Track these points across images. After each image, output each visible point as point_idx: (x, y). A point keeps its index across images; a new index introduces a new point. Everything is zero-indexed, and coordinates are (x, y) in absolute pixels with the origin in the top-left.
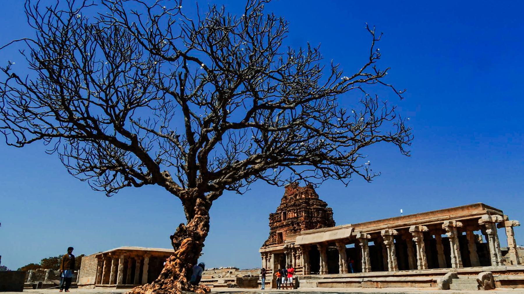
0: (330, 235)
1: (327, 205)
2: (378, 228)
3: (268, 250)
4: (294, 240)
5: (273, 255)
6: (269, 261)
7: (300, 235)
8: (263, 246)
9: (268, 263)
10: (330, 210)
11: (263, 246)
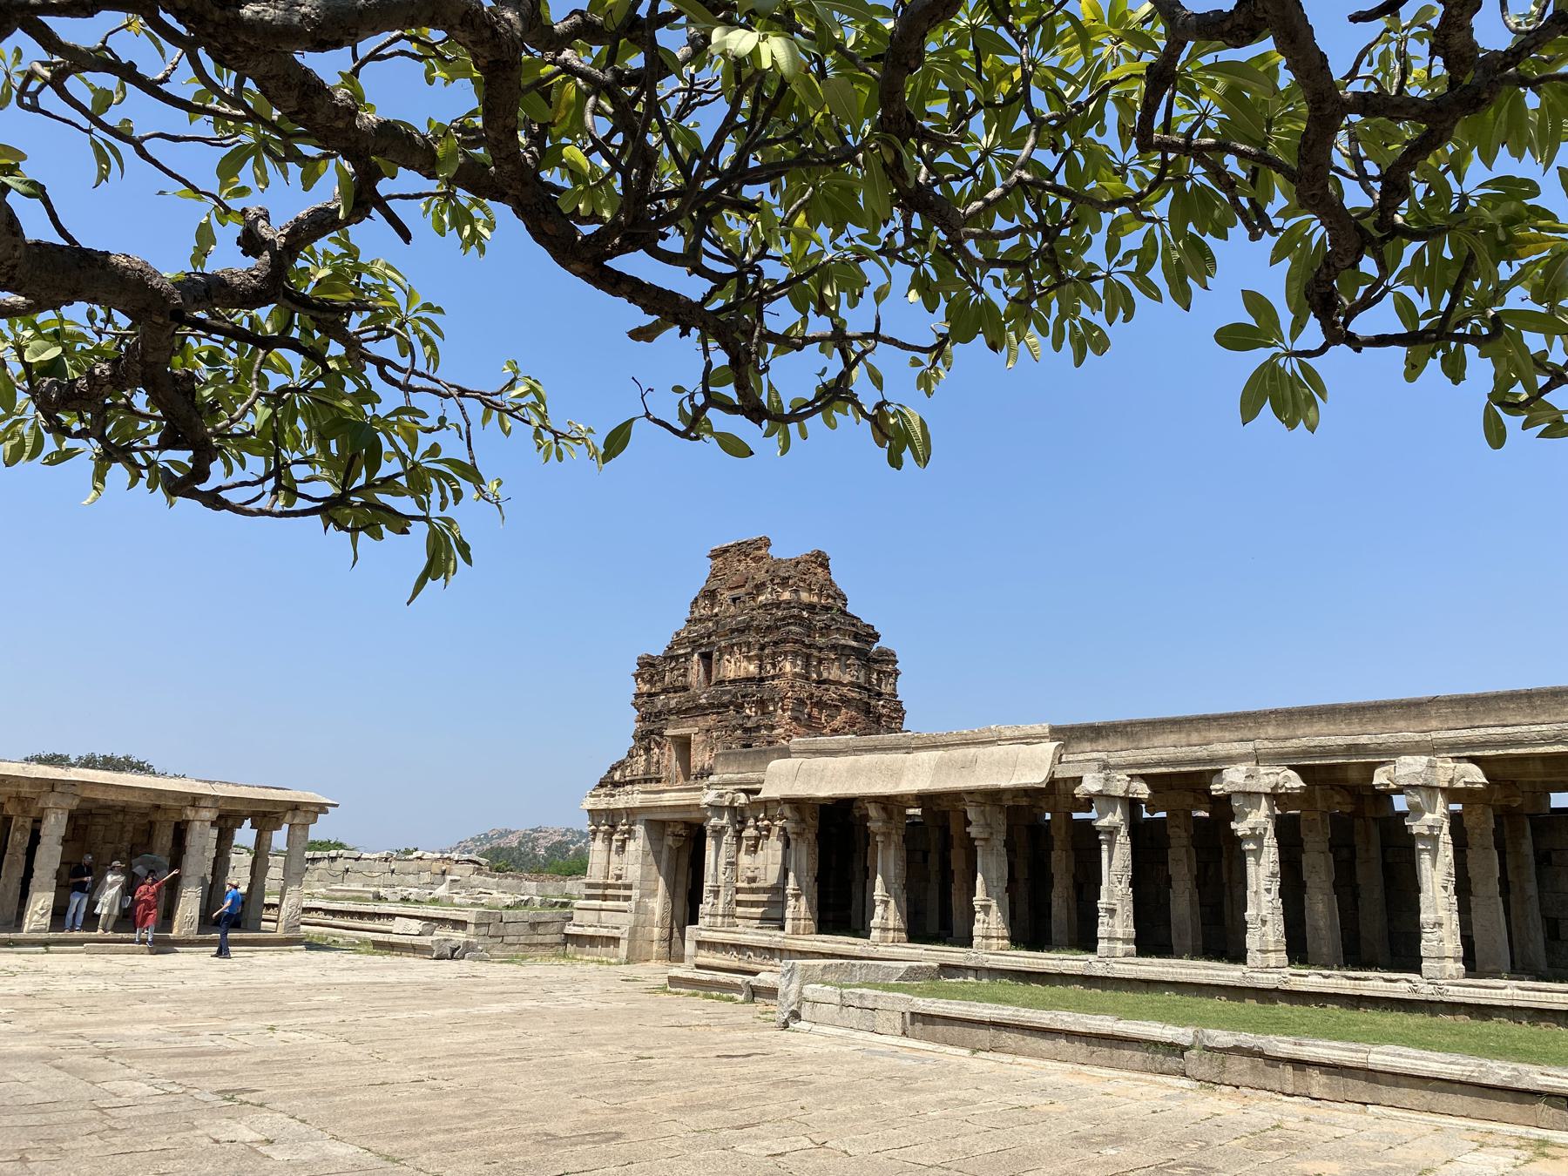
0: (939, 766)
1: (877, 637)
2: (1202, 752)
3: (621, 801)
4: (751, 775)
5: (640, 829)
6: (622, 848)
7: (786, 753)
8: (601, 785)
9: (614, 858)
10: (888, 657)
11: (601, 785)
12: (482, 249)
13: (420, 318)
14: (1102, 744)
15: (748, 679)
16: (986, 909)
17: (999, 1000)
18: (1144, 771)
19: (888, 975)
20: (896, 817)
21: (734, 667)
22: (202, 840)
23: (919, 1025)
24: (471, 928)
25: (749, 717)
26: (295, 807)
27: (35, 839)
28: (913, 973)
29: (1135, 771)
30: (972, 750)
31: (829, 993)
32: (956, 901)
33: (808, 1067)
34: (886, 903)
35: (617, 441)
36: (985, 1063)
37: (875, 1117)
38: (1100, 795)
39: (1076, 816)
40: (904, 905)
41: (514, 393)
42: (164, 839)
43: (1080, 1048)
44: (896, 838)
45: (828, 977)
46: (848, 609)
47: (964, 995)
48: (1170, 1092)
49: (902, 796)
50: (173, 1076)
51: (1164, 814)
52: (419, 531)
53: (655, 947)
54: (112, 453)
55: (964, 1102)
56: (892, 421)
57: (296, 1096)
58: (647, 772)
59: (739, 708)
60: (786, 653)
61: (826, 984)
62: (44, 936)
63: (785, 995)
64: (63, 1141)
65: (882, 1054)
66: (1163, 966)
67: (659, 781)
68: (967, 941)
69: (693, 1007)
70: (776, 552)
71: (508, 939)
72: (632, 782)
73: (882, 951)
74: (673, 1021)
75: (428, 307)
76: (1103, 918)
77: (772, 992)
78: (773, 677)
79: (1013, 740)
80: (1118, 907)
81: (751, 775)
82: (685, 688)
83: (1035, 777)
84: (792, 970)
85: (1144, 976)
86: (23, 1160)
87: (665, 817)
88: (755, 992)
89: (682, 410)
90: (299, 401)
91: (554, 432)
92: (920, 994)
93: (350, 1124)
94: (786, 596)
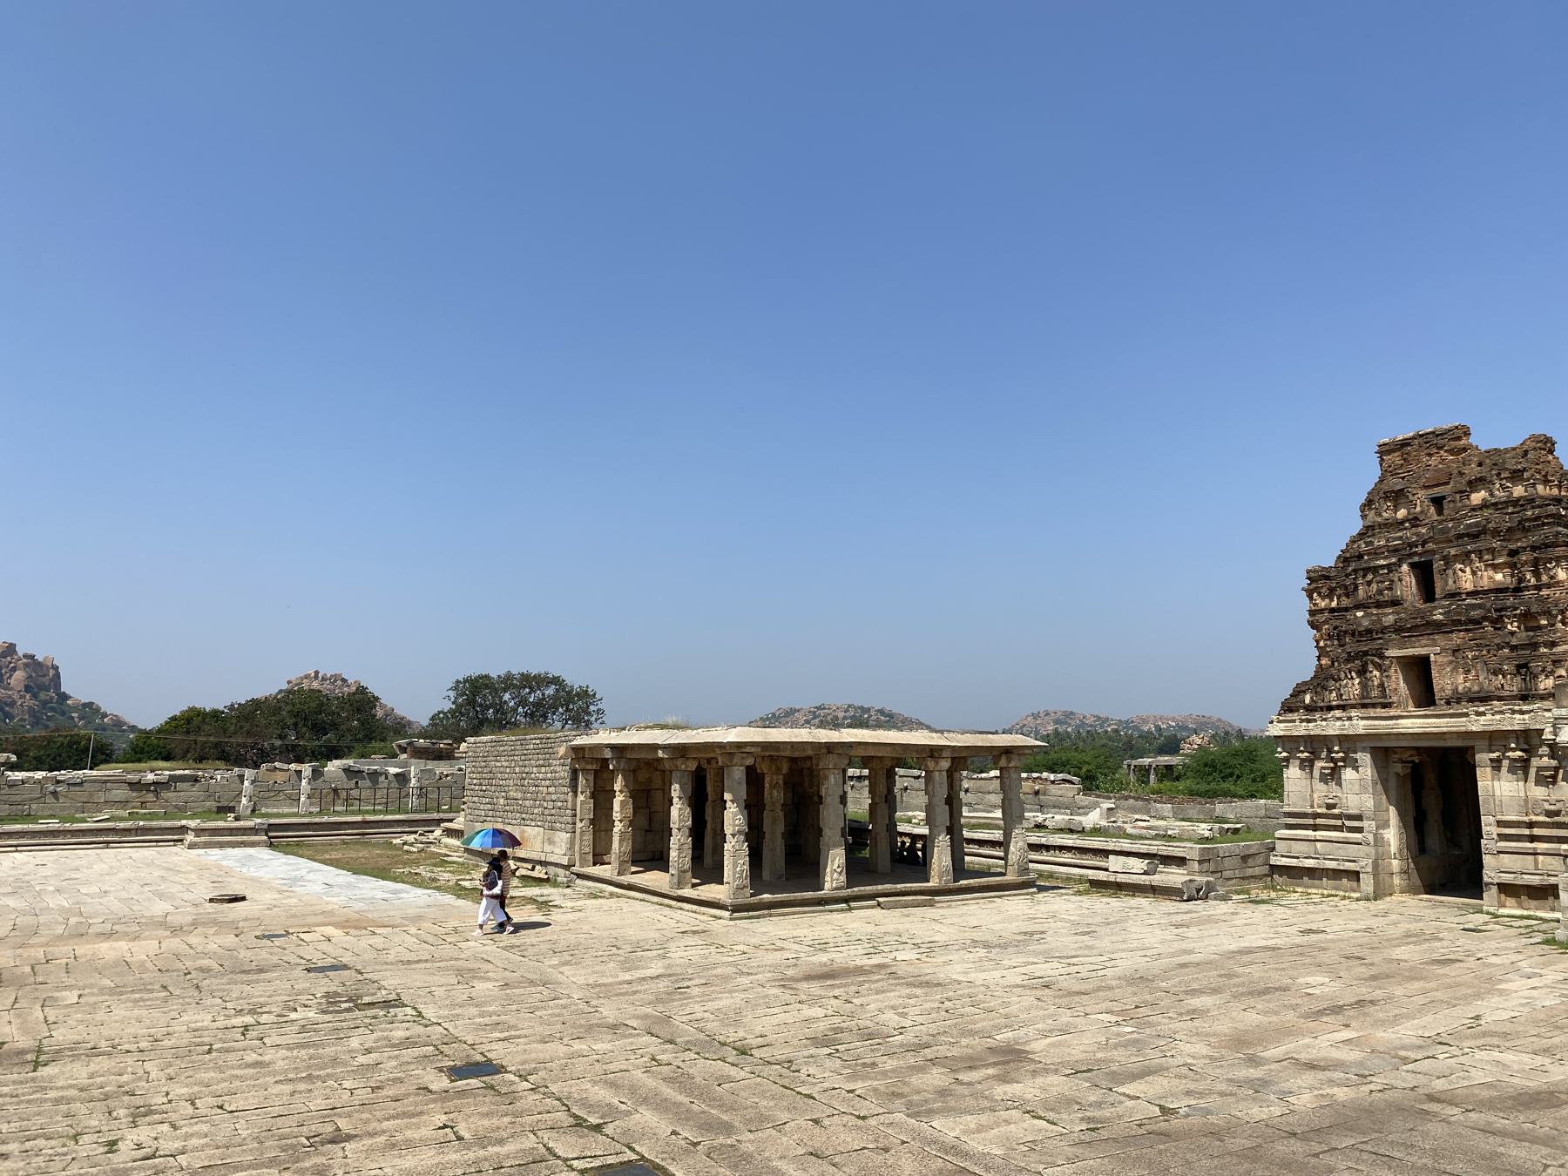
3: (1331, 726)
5: (1364, 758)
15: (1500, 590)
25: (1512, 633)
53: (1397, 880)
58: (1363, 698)
59: (1498, 623)
60: (1558, 560)
67: (1385, 706)
70: (1473, 440)
71: (1227, 874)
78: (1538, 588)
82: (1395, 603)
94: (1519, 491)
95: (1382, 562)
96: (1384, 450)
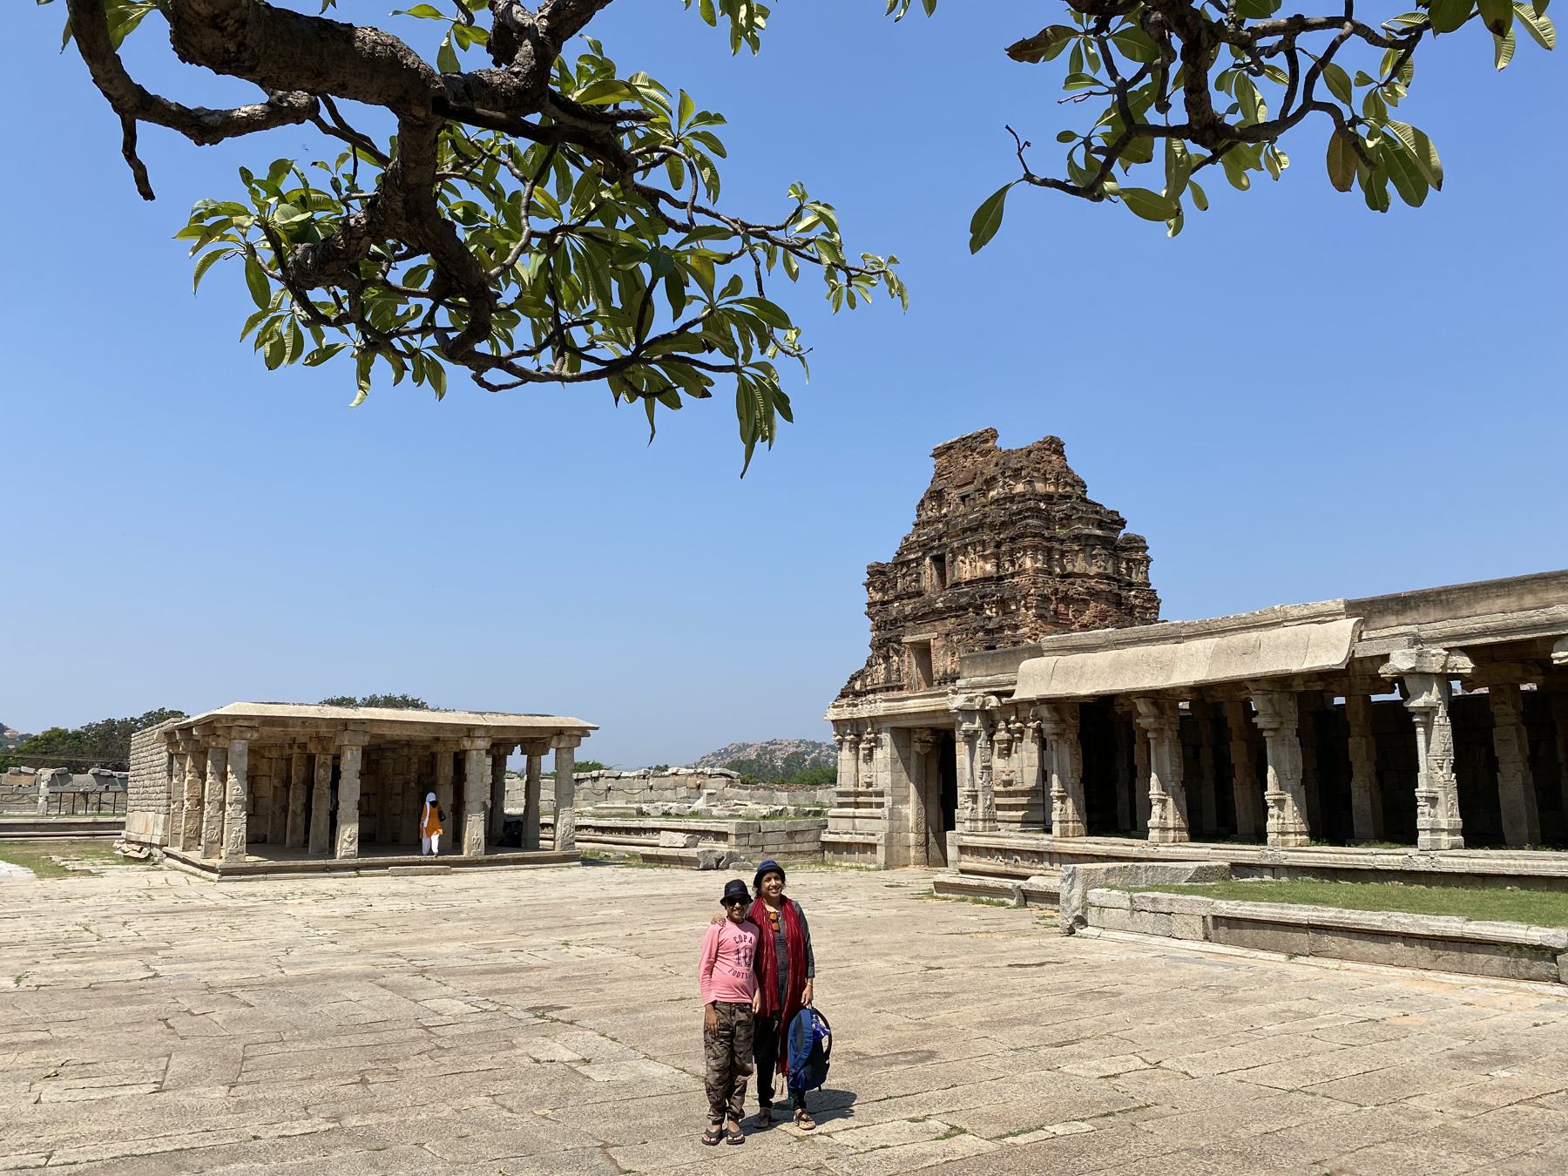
0: (1216, 654)
1: (1122, 523)
2: (1539, 616)
3: (865, 710)
4: (1001, 677)
5: (886, 737)
6: (870, 756)
7: (1038, 652)
8: (843, 696)
9: (862, 765)
10: (1137, 544)
11: (843, 696)
12: (755, 44)
13: (695, 135)
14: (1411, 616)
15: (986, 579)
16: (1280, 803)
17: (1314, 901)
18: (1459, 644)
19: (1176, 877)
20: (1169, 712)
21: (969, 568)
22: (479, 768)
23: (1223, 930)
24: (733, 839)
25: (990, 618)
26: (559, 732)
27: (336, 774)
28: (1203, 874)
29: (1453, 644)
30: (1254, 635)
31: (1117, 897)
32: (1240, 793)
33: (1111, 977)
34: (1164, 802)
35: (986, 222)
36: (1307, 969)
37: (1205, 1033)
38: (1412, 672)
39: (1375, 698)
40: (1183, 803)
41: (800, 226)
42: (446, 769)
43: (1423, 953)
44: (1170, 734)
45: (1112, 881)
46: (1088, 496)
47: (1271, 896)
48: (1544, 1001)
49: (1174, 689)
50: (487, 993)
51: (1484, 690)
52: (725, 387)
53: (912, 853)
54: (377, 342)
55: (1300, 1015)
56: (1370, 144)
57: (602, 1013)
58: (888, 680)
59: (979, 609)
60: (1025, 549)
61: (1112, 888)
62: (354, 861)
63: (1068, 900)
64: (397, 1060)
65: (1186, 960)
66: (1502, 858)
67: (901, 688)
68: (1260, 837)
69: (968, 914)
72: (873, 691)
73: (1163, 851)
74: (951, 929)
75: (704, 117)
76: (1423, 808)
77: (1052, 898)
78: (1013, 576)
79: (1301, 620)
80: (1441, 795)
81: (1001, 677)
82: (919, 594)
83: (1334, 658)
84: (1073, 875)
85: (1477, 870)
86: (364, 1082)
87: (910, 724)
88: (1027, 897)
89: (1072, 165)
90: (575, 242)
91: (847, 270)
92: (1220, 896)
93: (660, 1042)
94: (1020, 488)
95: (912, 556)
96: (938, 454)
